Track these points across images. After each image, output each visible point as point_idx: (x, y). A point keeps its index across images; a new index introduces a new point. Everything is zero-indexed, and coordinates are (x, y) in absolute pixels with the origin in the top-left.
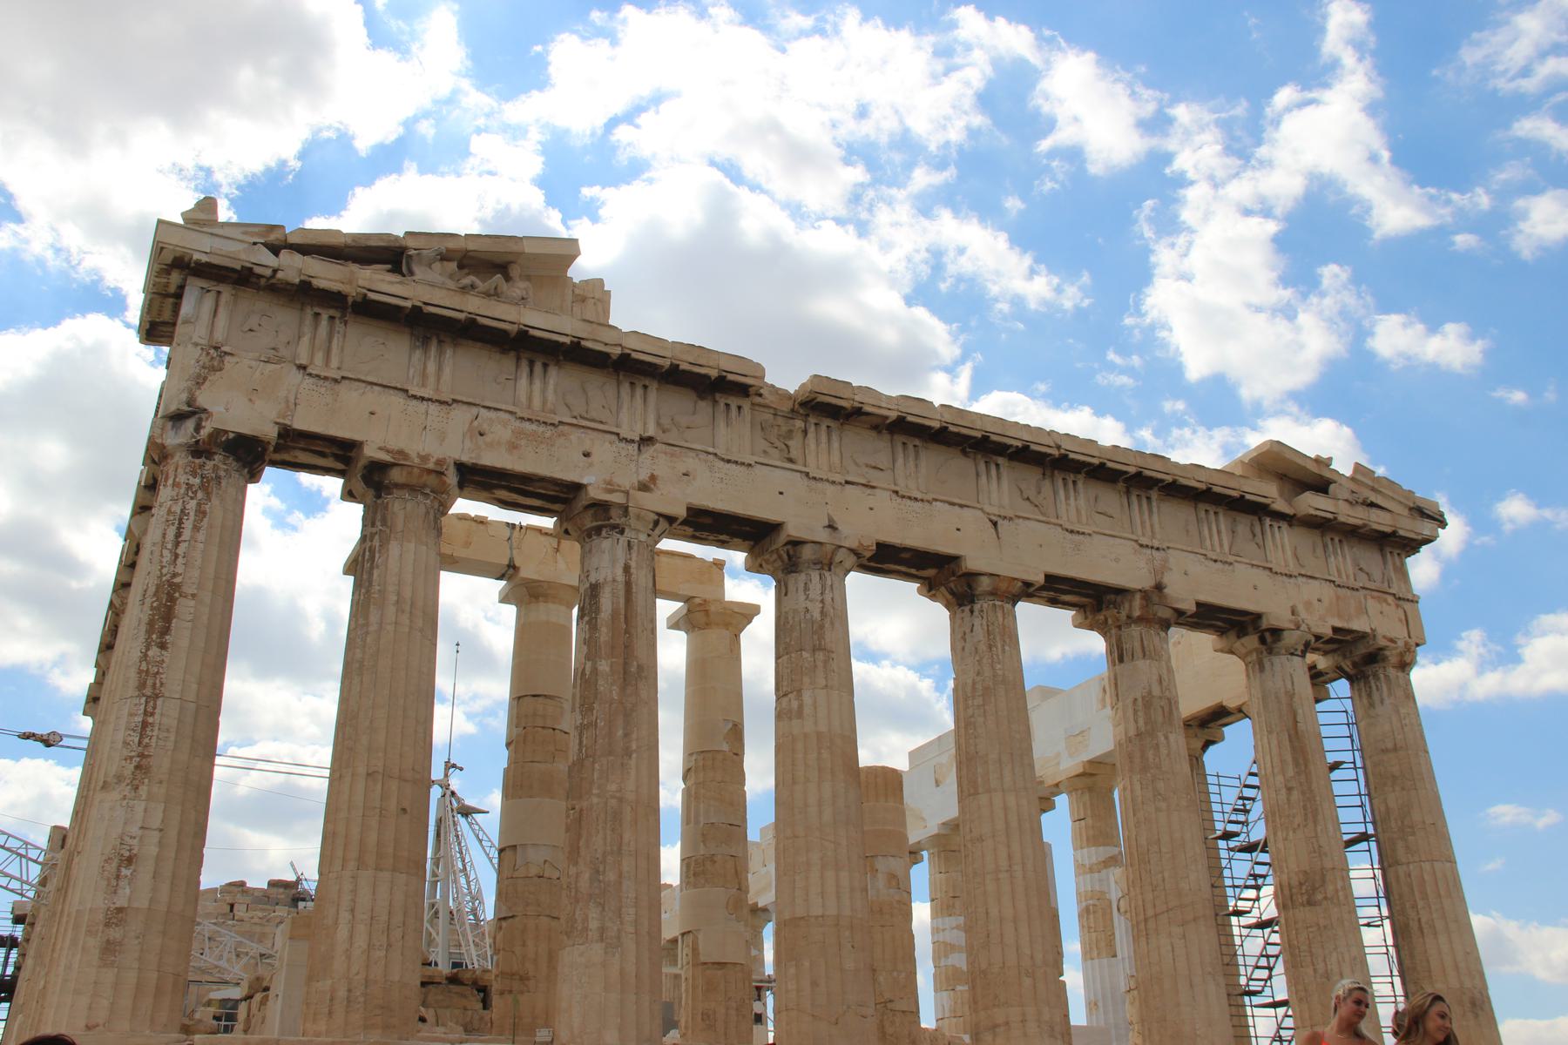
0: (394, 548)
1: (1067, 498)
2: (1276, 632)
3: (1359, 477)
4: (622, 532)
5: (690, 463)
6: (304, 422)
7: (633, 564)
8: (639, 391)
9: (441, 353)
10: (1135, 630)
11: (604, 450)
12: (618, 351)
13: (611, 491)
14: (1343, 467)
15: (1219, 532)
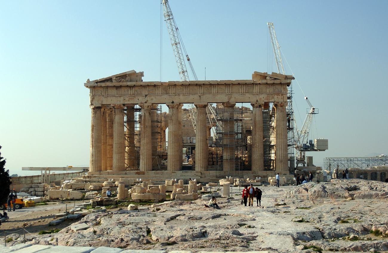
0: (116, 116)
1: (214, 89)
2: (253, 105)
3: (273, 74)
4: (144, 108)
5: (152, 97)
6: (104, 103)
7: (145, 113)
8: (145, 88)
9: (119, 90)
10: (226, 108)
11: (140, 98)
12: (140, 85)
13: (141, 104)
14: (270, 73)
15: (244, 89)
